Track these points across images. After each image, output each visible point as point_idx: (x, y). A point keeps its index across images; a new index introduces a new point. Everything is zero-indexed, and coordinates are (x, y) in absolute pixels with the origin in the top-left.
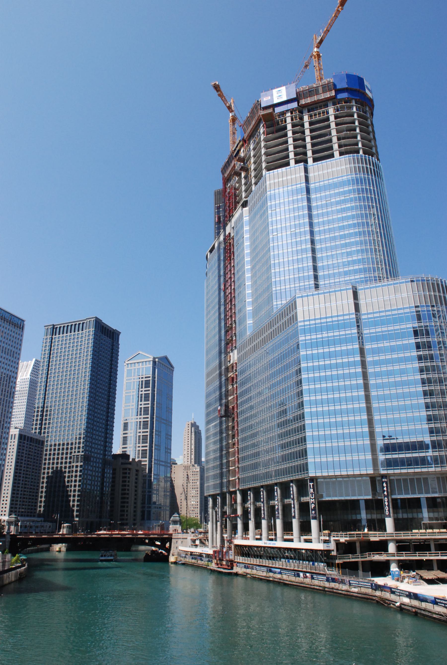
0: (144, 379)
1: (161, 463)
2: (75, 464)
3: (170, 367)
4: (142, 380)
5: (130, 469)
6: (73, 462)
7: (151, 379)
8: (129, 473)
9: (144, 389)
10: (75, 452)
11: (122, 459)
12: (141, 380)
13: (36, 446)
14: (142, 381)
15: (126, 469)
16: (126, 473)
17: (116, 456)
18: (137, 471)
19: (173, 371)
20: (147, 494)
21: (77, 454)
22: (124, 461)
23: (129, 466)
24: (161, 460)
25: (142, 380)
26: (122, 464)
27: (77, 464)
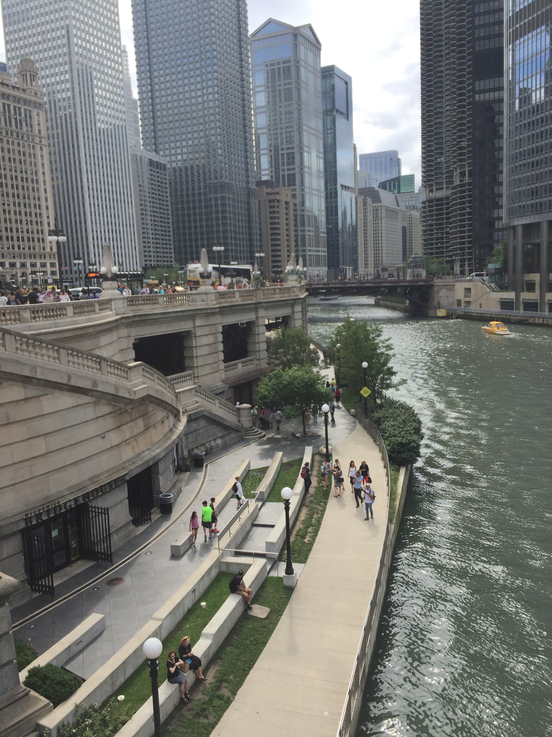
0: (282, 66)
2: (213, 196)
4: (279, 66)
5: (278, 201)
6: (210, 193)
7: (292, 63)
8: (278, 207)
9: (282, 82)
10: (210, 179)
11: (267, 187)
12: (276, 67)
13: (158, 172)
14: (279, 69)
15: (274, 201)
16: (274, 207)
17: (260, 183)
18: (287, 203)
20: (300, 233)
21: (214, 181)
22: (269, 190)
23: (277, 197)
24: (313, 187)
25: (279, 66)
26: (267, 194)
27: (216, 196)
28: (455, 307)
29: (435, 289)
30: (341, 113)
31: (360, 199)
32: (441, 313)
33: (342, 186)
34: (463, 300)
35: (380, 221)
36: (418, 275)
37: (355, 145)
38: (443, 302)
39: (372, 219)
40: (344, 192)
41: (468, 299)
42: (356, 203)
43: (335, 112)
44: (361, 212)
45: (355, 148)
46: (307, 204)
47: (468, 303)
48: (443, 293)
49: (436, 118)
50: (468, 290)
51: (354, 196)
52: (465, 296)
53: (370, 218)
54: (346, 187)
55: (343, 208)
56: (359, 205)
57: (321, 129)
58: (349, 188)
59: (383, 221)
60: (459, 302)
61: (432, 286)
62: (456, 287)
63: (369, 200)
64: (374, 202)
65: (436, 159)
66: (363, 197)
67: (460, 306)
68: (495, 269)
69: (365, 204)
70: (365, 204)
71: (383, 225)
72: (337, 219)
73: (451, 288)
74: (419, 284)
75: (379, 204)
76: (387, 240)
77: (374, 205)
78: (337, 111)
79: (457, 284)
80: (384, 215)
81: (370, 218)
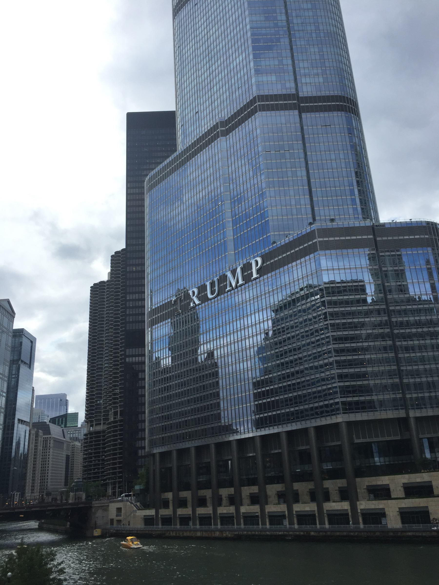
3: (12, 313)
28: (109, 526)
29: (93, 510)
31: (33, 432)
32: (97, 532)
33: (19, 420)
34: (116, 518)
36: (79, 498)
37: (33, 388)
38: (100, 522)
39: (42, 448)
40: (20, 425)
41: (119, 518)
42: (30, 435)
44: (32, 443)
45: (33, 390)
47: (119, 521)
48: (99, 513)
49: (97, 372)
50: (119, 510)
51: (28, 428)
52: (117, 516)
53: (40, 448)
54: (22, 421)
55: (18, 438)
56: (31, 436)
58: (25, 421)
59: (51, 450)
60: (112, 520)
61: (91, 507)
62: (110, 507)
64: (44, 434)
65: (97, 401)
67: (113, 525)
68: (140, 489)
69: (37, 435)
70: (37, 435)
71: (51, 453)
72: (12, 448)
73: (106, 509)
74: (79, 506)
75: (49, 436)
77: (44, 436)
79: (110, 504)
80: (52, 445)
81: (40, 448)
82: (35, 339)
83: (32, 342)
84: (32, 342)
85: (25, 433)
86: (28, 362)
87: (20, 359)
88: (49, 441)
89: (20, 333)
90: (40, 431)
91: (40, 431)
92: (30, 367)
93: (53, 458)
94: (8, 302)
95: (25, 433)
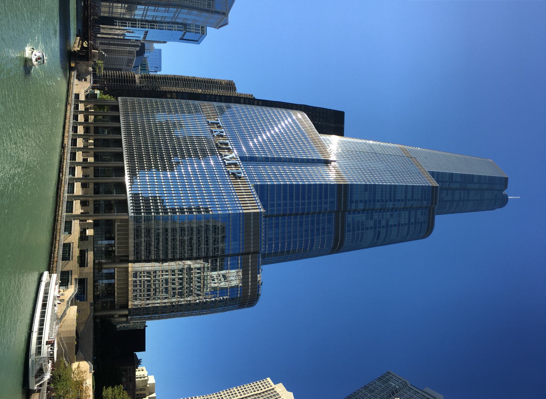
1: (145, 12)
3: (219, 26)
19: (215, 28)
24: (148, 12)
30: (184, 35)
35: (126, 55)
43: (185, 31)
45: (165, 42)
46: (139, 7)
57: (175, 10)
58: (146, 36)
63: (138, 49)
64: (137, 51)
66: (140, 45)
69: (136, 46)
70: (136, 46)
76: (113, 58)
78: (185, 33)
80: (129, 57)
82: (199, 44)
83: (197, 41)
84: (197, 41)
85: (139, 37)
86: (184, 38)
87: (187, 31)
88: (132, 55)
89: (204, 33)
90: (139, 48)
91: (139, 48)
92: (181, 39)
93: (121, 59)
94: (226, 24)
95: (139, 37)
